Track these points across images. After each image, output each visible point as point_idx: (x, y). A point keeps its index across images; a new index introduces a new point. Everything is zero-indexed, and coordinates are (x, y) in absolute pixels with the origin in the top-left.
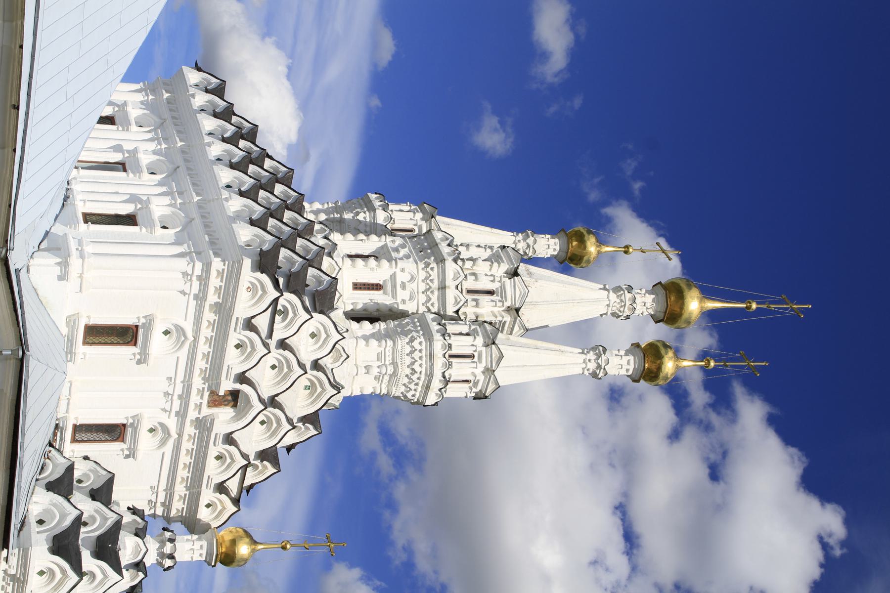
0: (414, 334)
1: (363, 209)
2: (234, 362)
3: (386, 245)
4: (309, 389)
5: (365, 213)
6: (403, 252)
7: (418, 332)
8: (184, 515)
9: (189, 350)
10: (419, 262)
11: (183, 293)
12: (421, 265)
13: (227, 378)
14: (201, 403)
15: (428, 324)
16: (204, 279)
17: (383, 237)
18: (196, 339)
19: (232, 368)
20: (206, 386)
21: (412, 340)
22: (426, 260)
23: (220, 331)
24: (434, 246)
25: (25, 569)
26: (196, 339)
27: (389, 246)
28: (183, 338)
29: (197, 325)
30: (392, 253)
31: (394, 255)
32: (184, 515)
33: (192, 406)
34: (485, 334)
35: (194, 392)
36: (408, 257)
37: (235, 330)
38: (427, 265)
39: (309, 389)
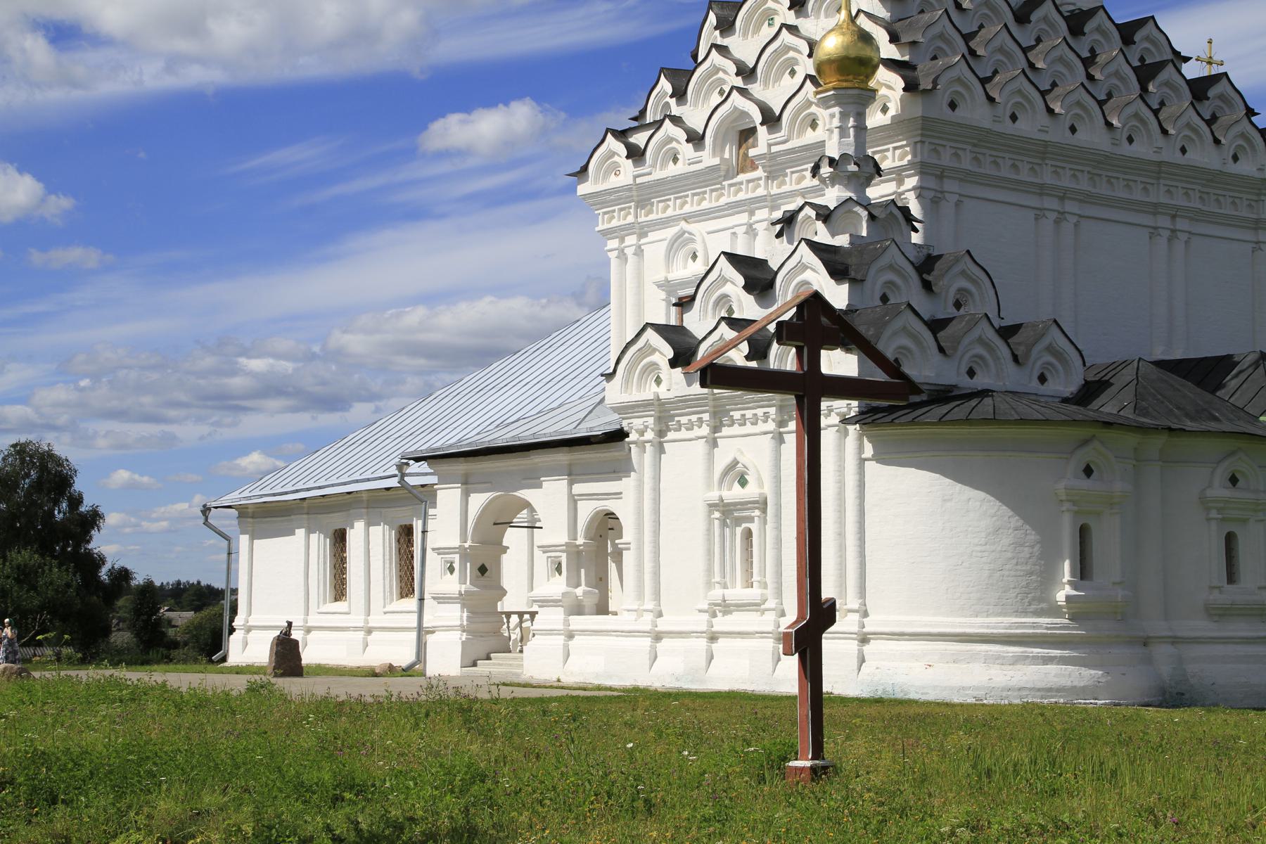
2: (690, 159)
4: (772, 19)
8: (904, 143)
9: (699, 221)
11: (639, 252)
13: (701, 161)
14: (749, 181)
16: (619, 233)
18: (687, 218)
19: (689, 160)
20: (726, 183)
23: (664, 190)
25: (638, 406)
26: (687, 218)
28: (686, 235)
29: (668, 222)
32: (904, 143)
33: (761, 192)
35: (742, 196)
37: (650, 174)
39: (772, 19)
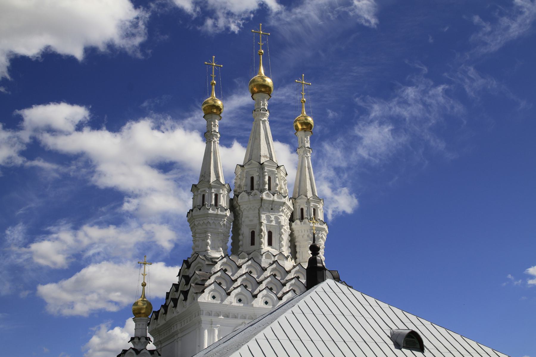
0: (320, 235)
1: (222, 221)
3: (266, 224)
5: (225, 220)
6: (273, 217)
7: (319, 233)
10: (279, 214)
12: (281, 214)
15: (317, 227)
17: (263, 224)
21: (322, 238)
22: (280, 210)
24: (273, 203)
27: (266, 223)
30: (271, 224)
31: (274, 223)
34: (316, 202)
36: (277, 219)
38: (283, 211)
